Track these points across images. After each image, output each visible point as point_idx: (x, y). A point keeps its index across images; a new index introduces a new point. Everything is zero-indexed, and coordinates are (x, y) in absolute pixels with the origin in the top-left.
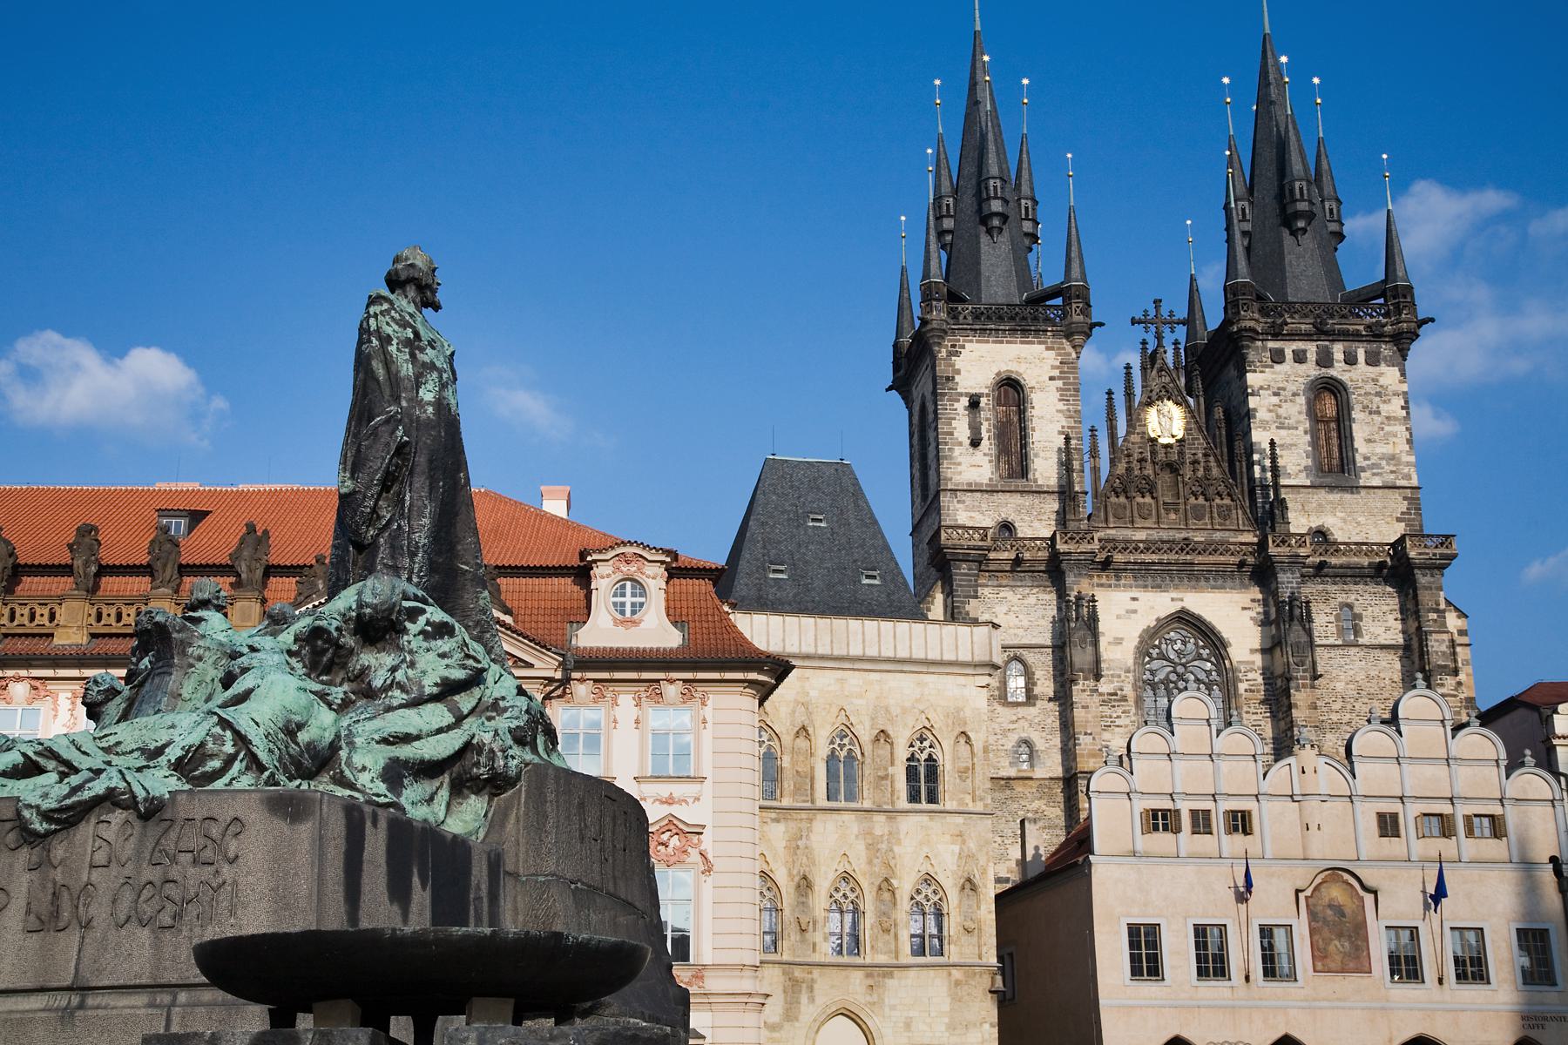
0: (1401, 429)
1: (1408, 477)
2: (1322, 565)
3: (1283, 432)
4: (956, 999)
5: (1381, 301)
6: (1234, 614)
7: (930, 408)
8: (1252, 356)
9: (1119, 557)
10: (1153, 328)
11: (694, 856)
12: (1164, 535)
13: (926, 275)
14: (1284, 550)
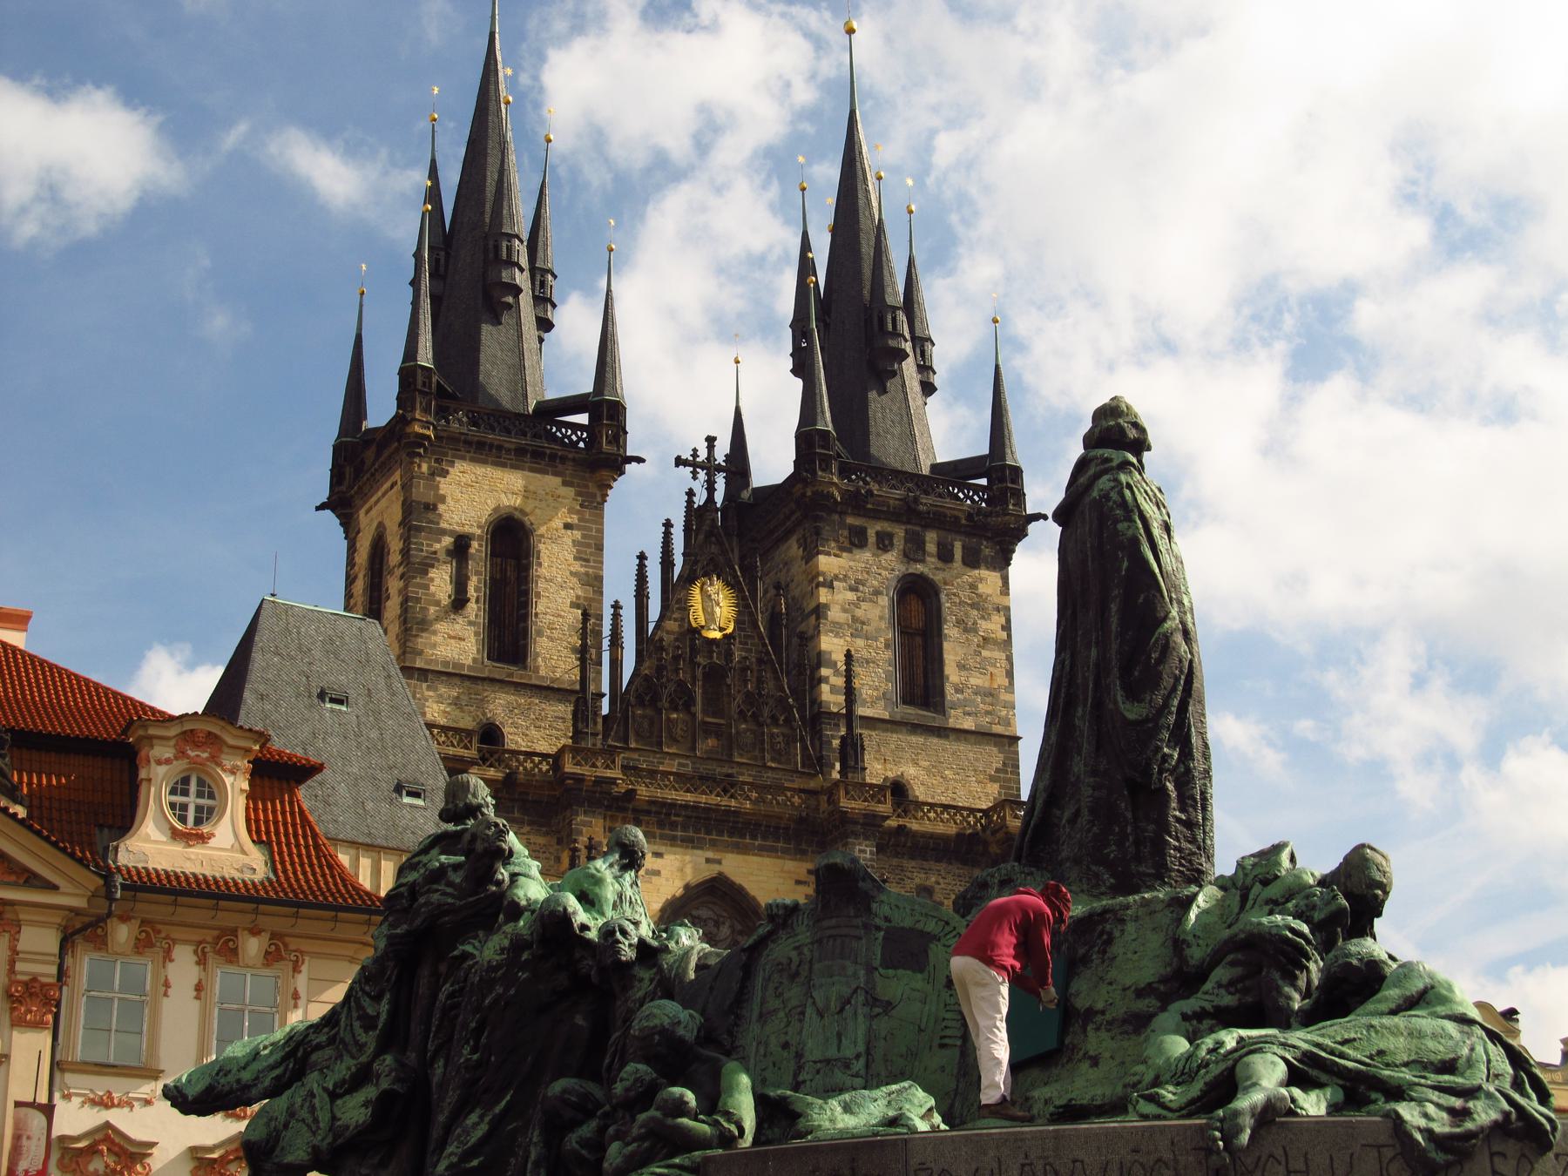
1: (1007, 722)
3: (860, 642)
5: (983, 482)
7: (395, 544)
8: (826, 530)
9: (643, 792)
10: (702, 475)
12: (704, 768)
13: (411, 351)
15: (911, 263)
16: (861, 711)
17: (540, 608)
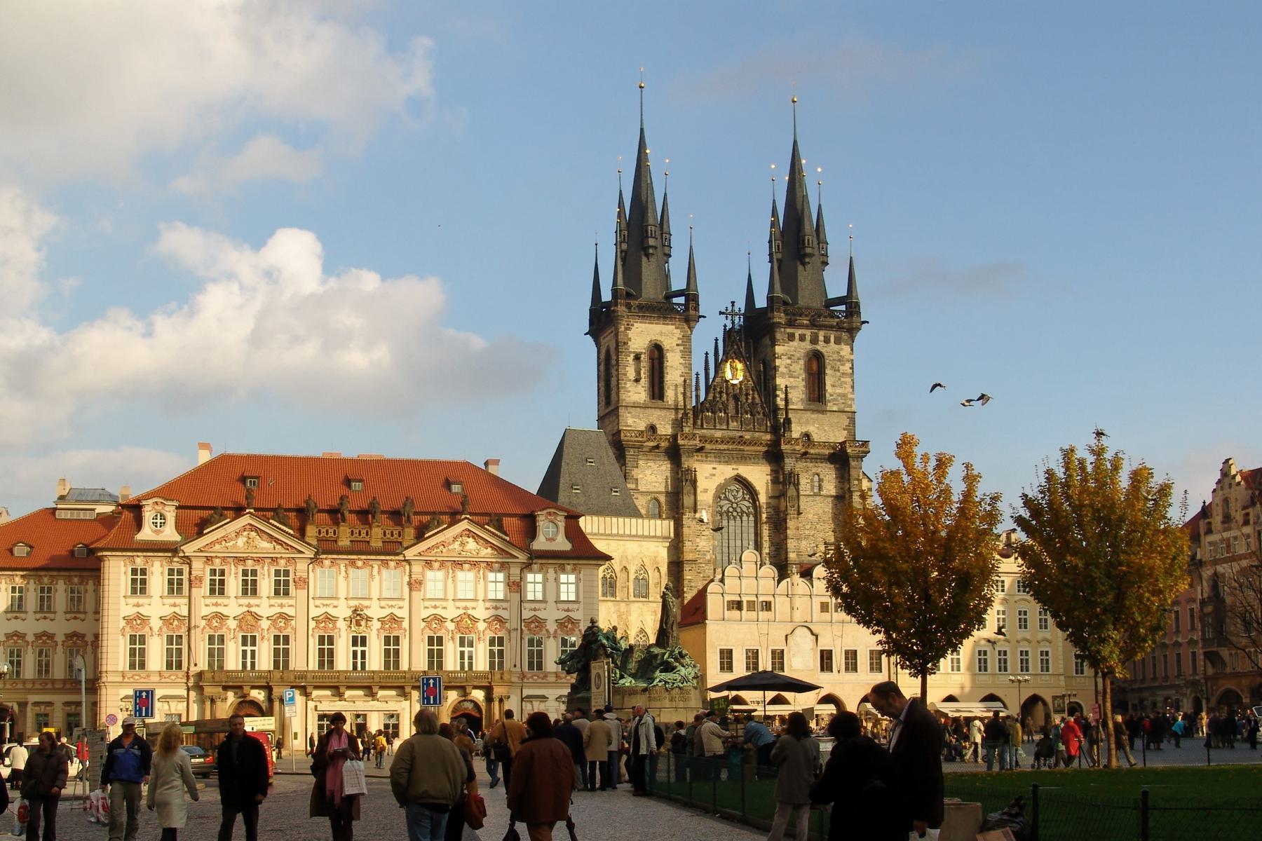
1: (850, 406)
2: (806, 453)
5: (843, 308)
6: (759, 475)
7: (614, 357)
8: (778, 336)
9: (708, 446)
12: (731, 434)
15: (820, 207)
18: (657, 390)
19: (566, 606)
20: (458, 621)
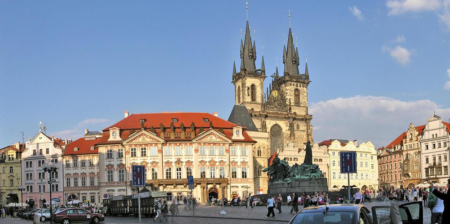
0: (306, 98)
1: (307, 105)
4: (263, 181)
5: (304, 77)
7: (241, 88)
11: (247, 165)
12: (275, 112)
14: (291, 116)
16: (291, 104)
17: (257, 95)
18: (253, 99)
19: (243, 157)
20: (210, 162)
